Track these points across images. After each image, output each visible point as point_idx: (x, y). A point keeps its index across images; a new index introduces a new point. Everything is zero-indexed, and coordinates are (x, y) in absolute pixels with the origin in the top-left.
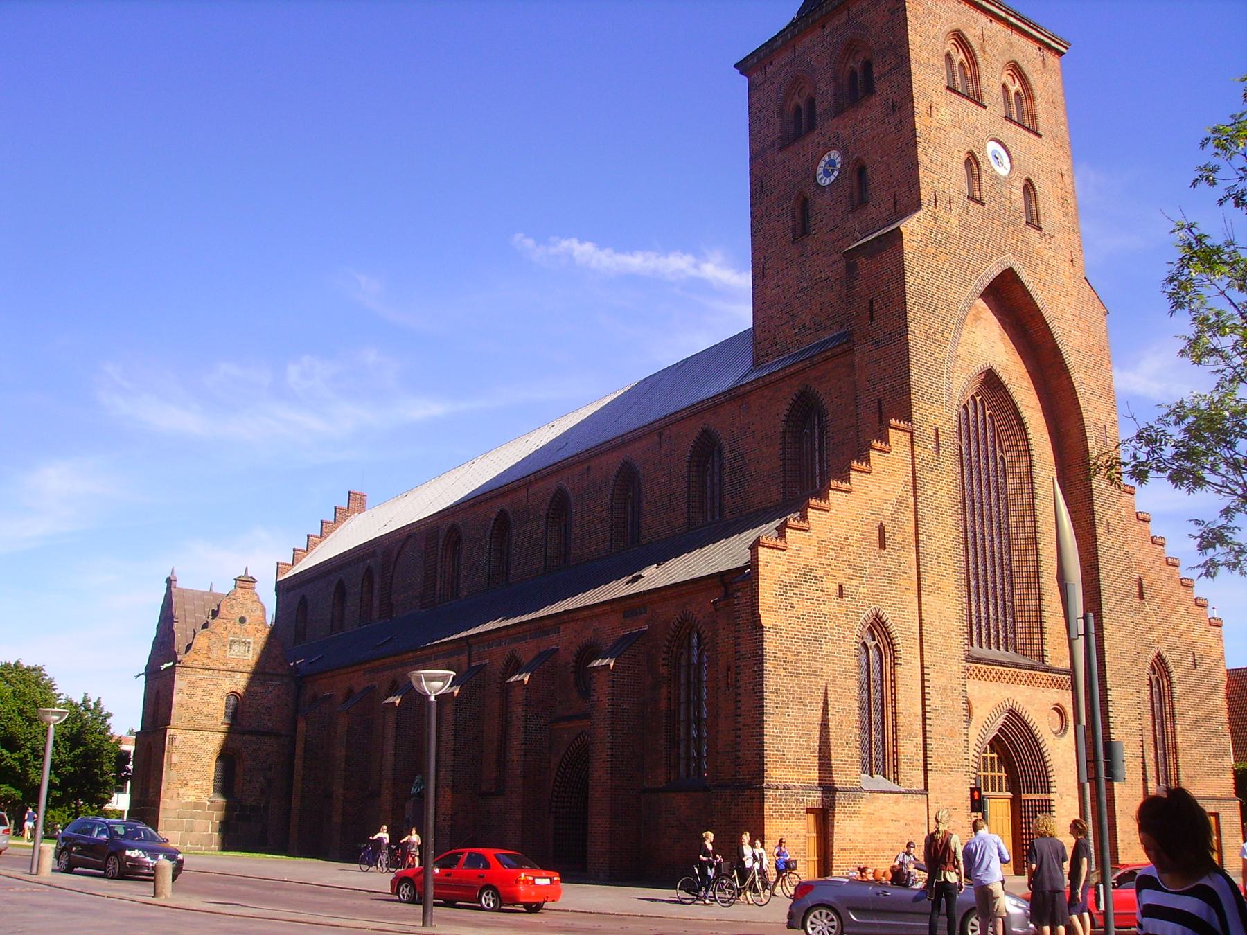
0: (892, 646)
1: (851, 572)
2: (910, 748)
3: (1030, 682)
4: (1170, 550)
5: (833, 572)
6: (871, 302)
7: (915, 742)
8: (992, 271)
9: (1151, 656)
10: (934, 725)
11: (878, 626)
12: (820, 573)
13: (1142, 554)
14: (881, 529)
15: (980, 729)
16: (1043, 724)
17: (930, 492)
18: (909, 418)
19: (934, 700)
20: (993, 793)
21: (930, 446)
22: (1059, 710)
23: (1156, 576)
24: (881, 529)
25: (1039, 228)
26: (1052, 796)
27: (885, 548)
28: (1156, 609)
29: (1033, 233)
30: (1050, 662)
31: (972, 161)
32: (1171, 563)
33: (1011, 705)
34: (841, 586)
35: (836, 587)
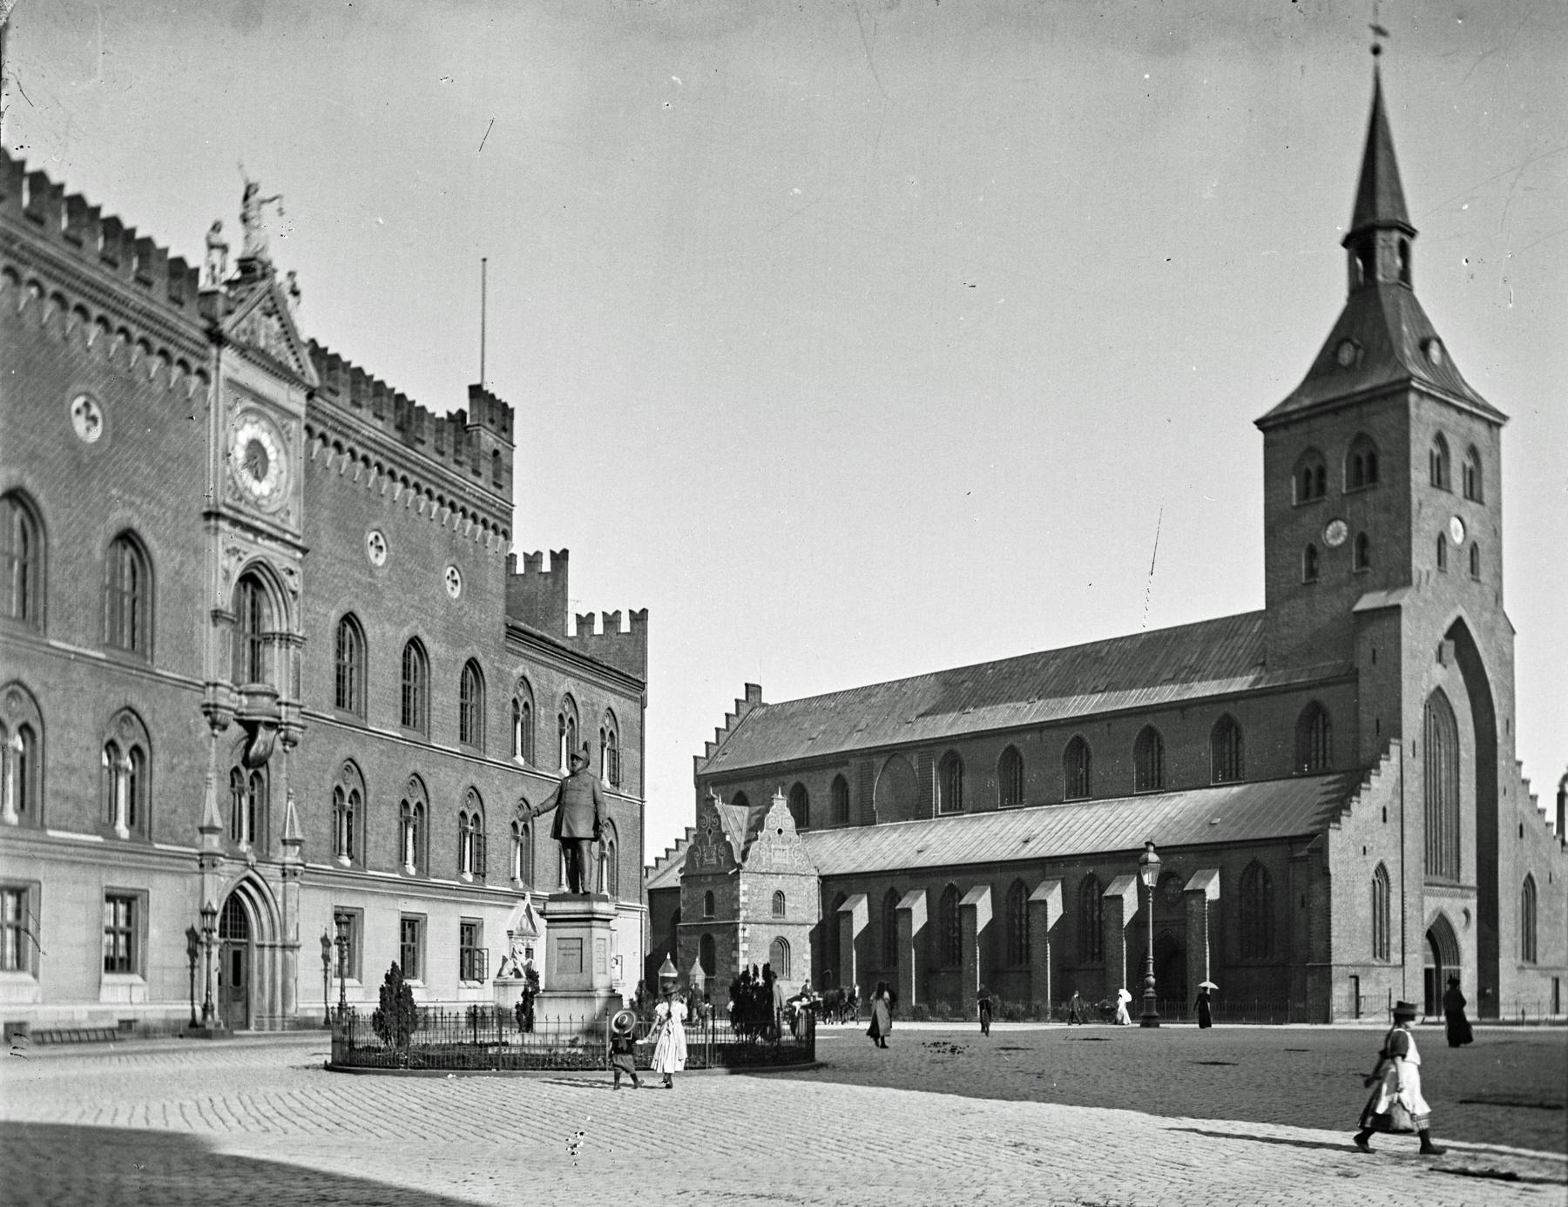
0: (1387, 880)
2: (1395, 940)
3: (1453, 896)
4: (1540, 804)
6: (1374, 651)
8: (1448, 622)
9: (1524, 876)
10: (1408, 925)
11: (1381, 869)
13: (1523, 806)
16: (1457, 921)
18: (1399, 736)
19: (1407, 914)
22: (1466, 913)
23: (1532, 821)
25: (1478, 581)
29: (1475, 586)
30: (1463, 882)
31: (1442, 540)
32: (1542, 812)
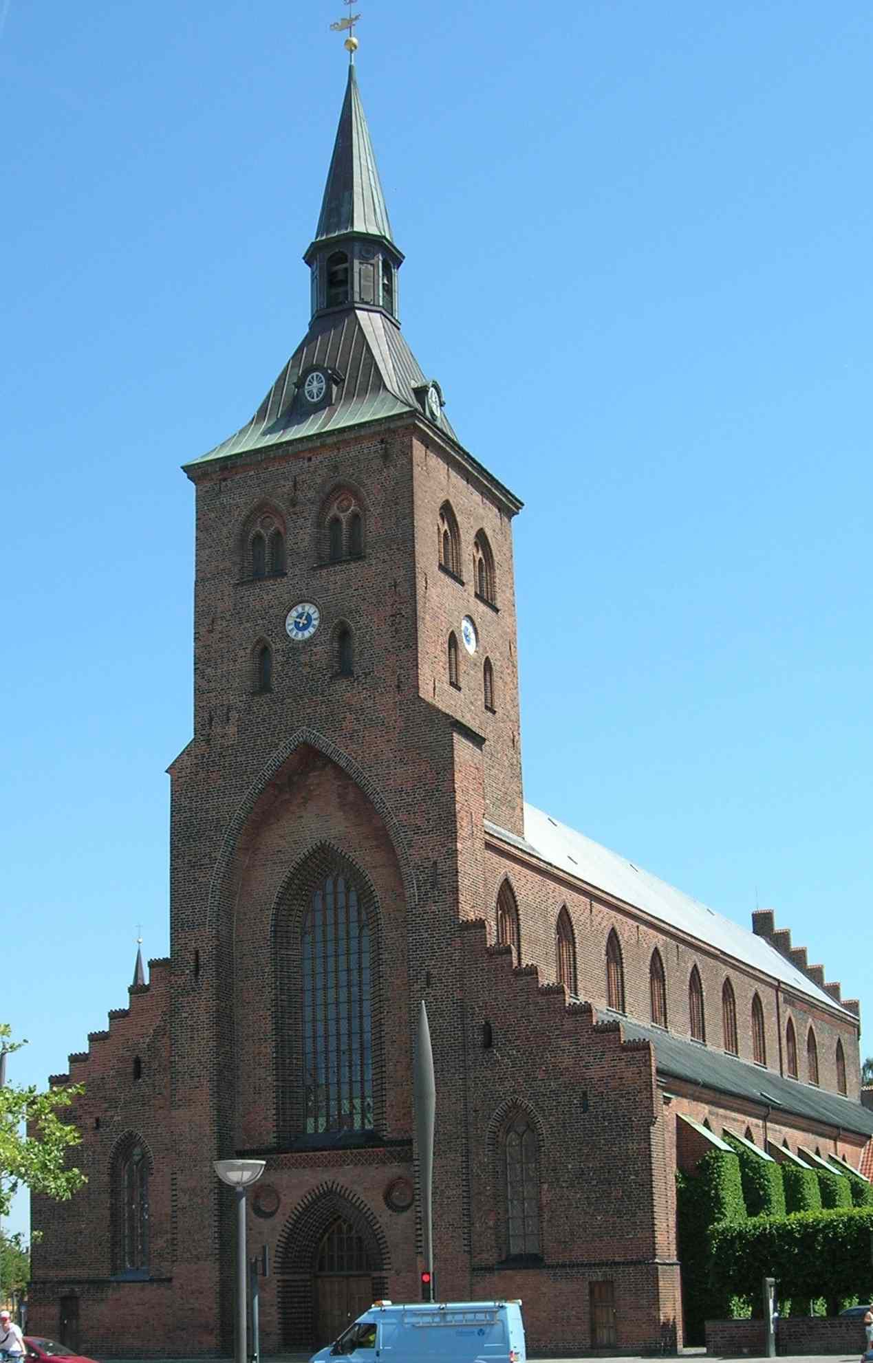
1: (106, 1105)
5: (91, 1110)
7: (164, 1239)
12: (79, 1113)
14: (138, 1062)
15: (287, 1217)
17: (184, 1015)
20: (331, 1273)
21: (188, 972)
24: (138, 1062)
26: (384, 1274)
27: (139, 1077)
28: (515, 1053)
33: (330, 1186)
34: (97, 1120)
35: (93, 1120)
